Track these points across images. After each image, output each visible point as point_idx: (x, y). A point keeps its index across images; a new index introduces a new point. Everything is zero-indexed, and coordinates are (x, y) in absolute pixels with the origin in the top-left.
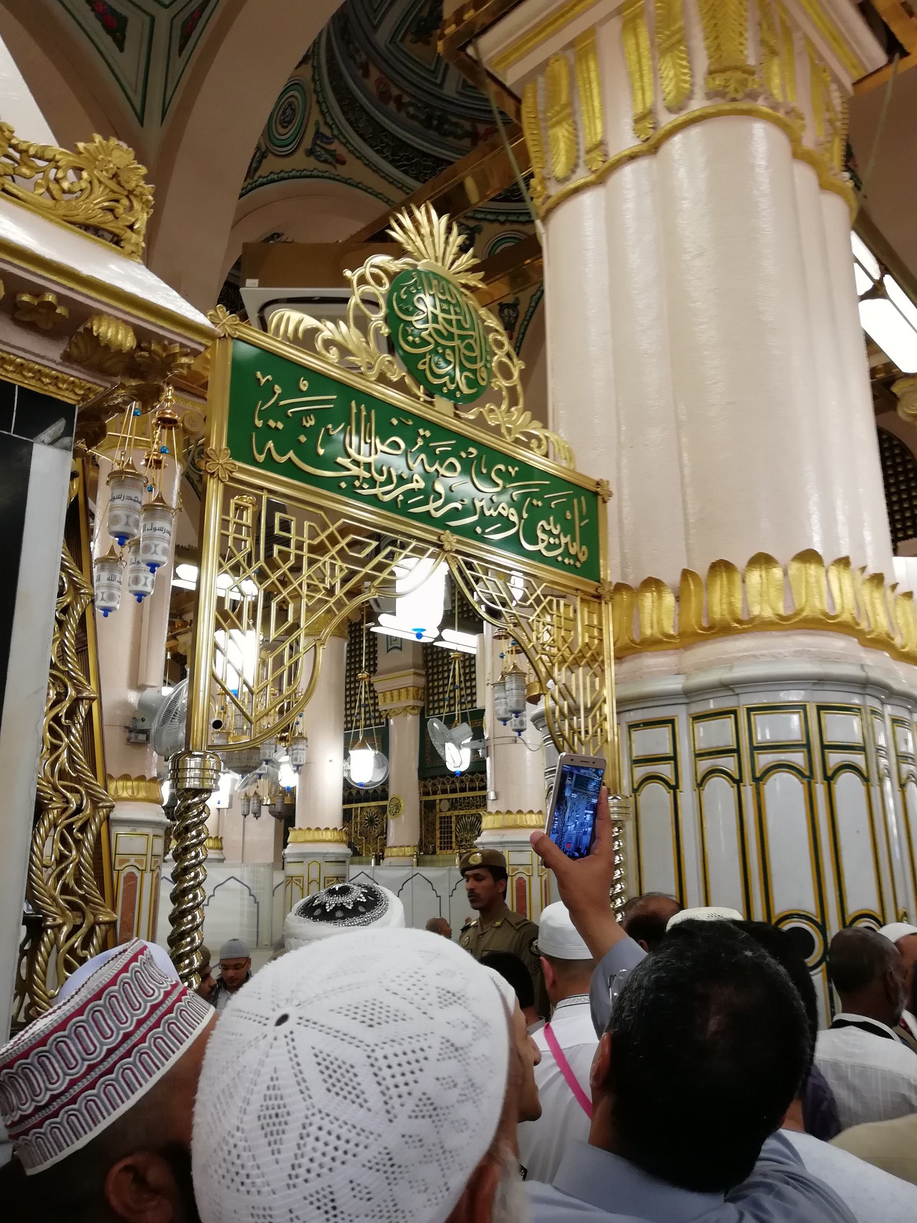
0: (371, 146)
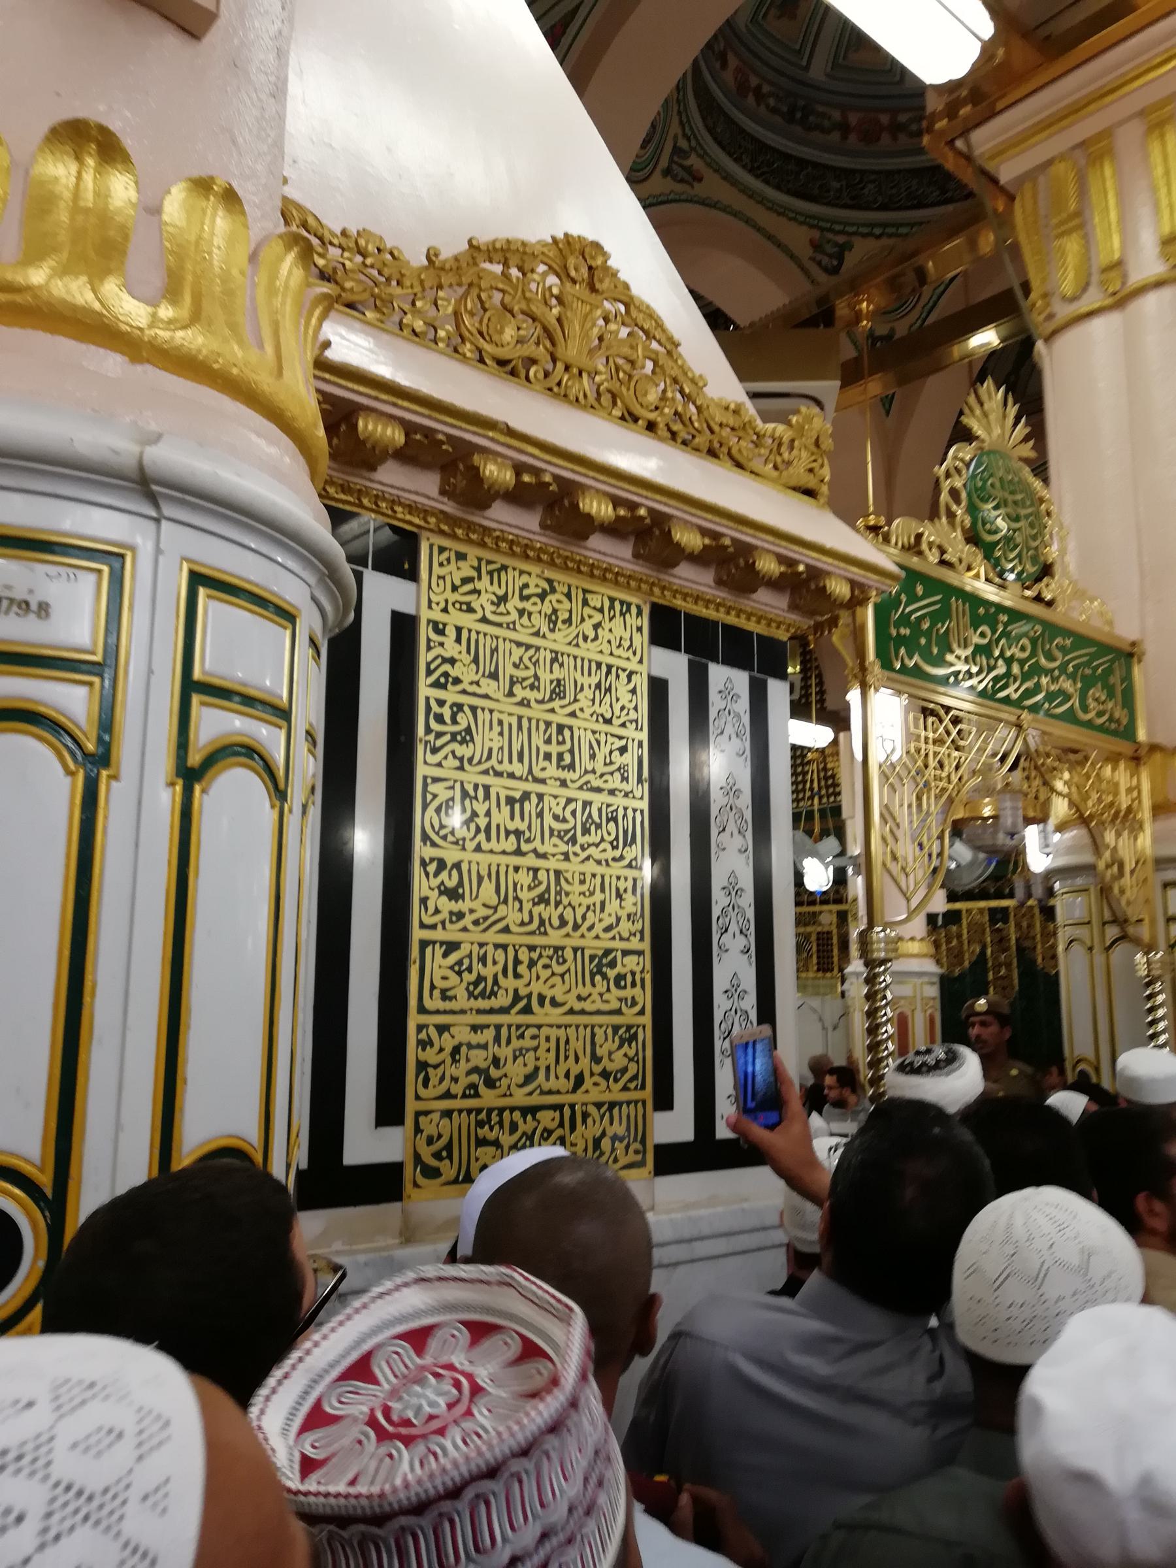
0: (730, 154)
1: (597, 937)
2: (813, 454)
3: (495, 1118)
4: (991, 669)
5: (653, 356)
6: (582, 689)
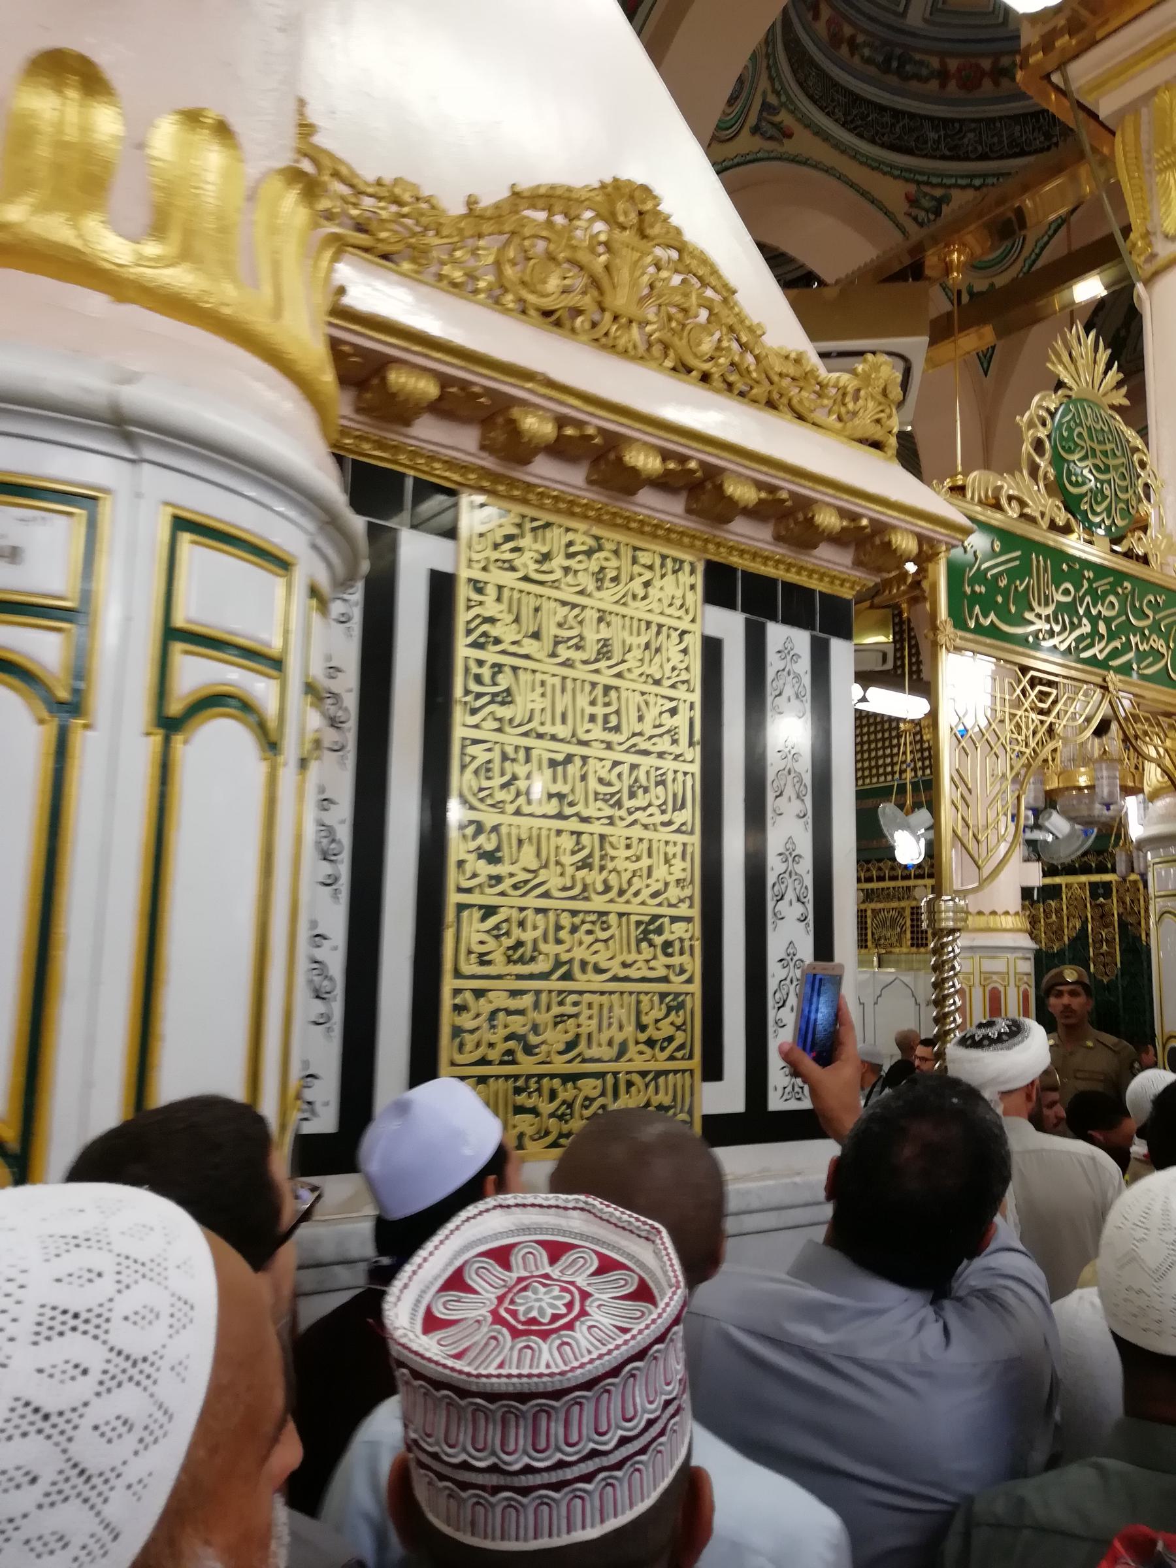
0: (822, 108)
1: (643, 903)
2: (880, 404)
4: (1074, 626)
5: (707, 304)
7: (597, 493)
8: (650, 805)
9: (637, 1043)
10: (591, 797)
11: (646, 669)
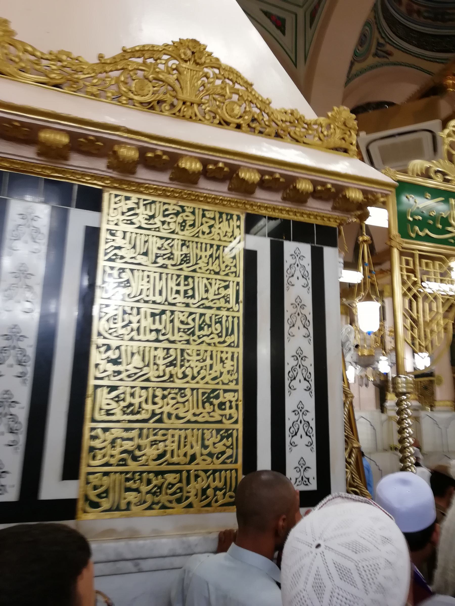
1: (207, 383)
3: (137, 476)
5: (236, 92)
6: (201, 258)
7: (177, 185)
8: (212, 333)
9: (202, 455)
10: (176, 331)
11: (210, 267)
